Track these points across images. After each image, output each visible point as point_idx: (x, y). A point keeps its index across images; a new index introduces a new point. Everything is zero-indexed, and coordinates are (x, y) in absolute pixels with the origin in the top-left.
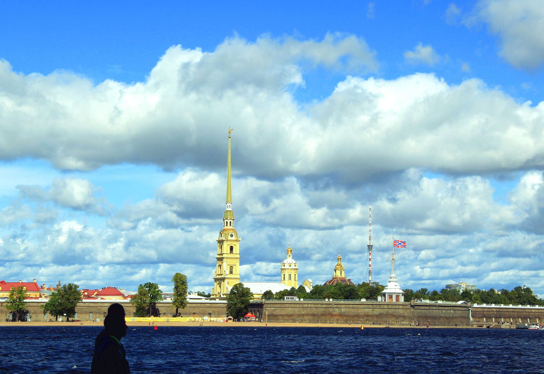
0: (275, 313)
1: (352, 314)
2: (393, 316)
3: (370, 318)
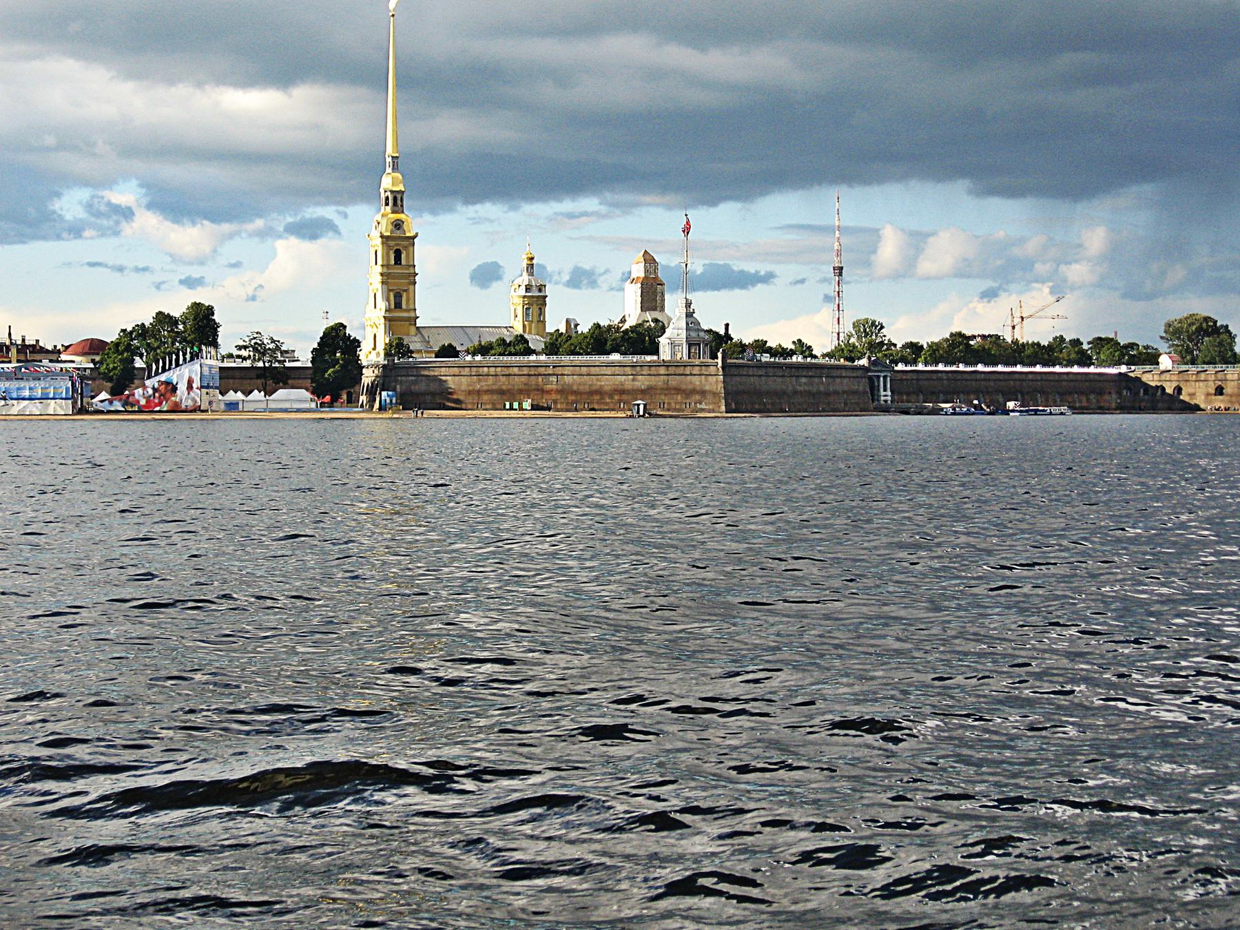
0: (415, 388)
1: (587, 388)
2: (678, 390)
3: (625, 397)
